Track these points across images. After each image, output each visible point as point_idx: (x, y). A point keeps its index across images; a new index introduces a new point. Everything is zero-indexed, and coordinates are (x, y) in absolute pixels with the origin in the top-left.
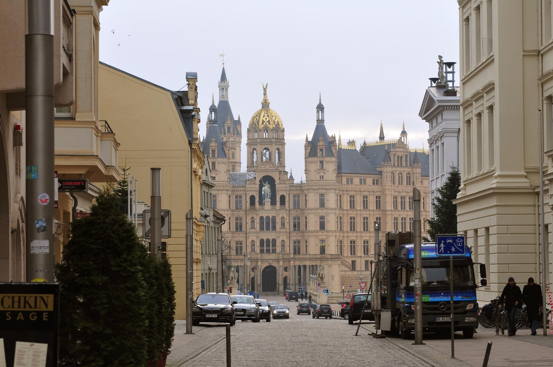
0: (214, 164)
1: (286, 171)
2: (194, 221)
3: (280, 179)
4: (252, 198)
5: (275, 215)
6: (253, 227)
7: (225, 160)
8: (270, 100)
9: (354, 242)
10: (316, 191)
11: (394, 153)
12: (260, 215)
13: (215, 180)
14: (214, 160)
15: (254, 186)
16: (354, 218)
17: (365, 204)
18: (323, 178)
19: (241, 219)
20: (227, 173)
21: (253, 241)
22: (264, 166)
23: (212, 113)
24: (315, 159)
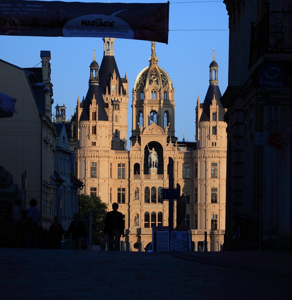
0: (95, 129)
1: (175, 137)
2: (43, 184)
4: (137, 166)
7: (106, 123)
12: (145, 186)
13: (95, 145)
18: (216, 145)
23: (93, 71)
24: (206, 123)
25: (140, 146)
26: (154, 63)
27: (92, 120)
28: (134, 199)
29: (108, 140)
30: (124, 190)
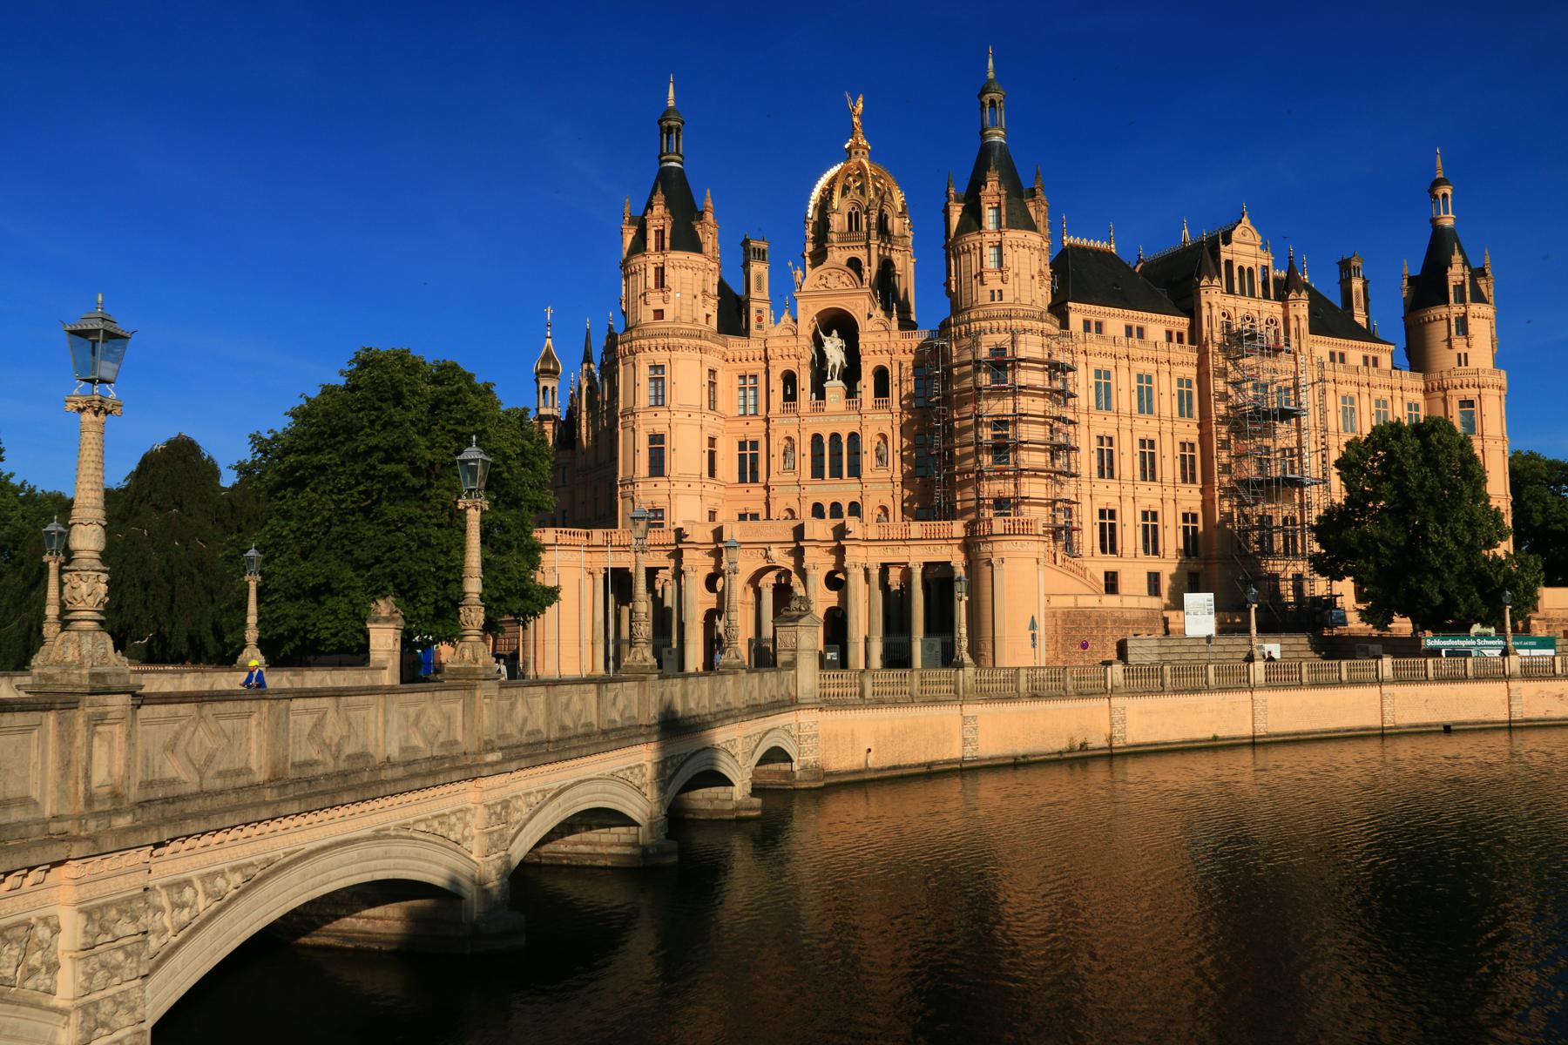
0: (660, 273)
3: (870, 316)
4: (790, 379)
9: (1112, 514)
11: (1229, 257)
15: (793, 341)
16: (1110, 439)
17: (1146, 401)
19: (754, 445)
20: (704, 301)
22: (824, 281)
24: (972, 239)
25: (794, 324)
26: (856, 153)
27: (653, 250)
28: (781, 469)
29: (701, 304)
30: (754, 445)
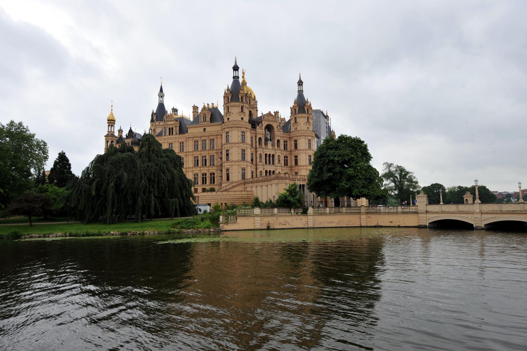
0: (242, 107)
3: (277, 128)
5: (274, 153)
6: (261, 161)
8: (246, 81)
10: (306, 137)
12: (265, 153)
14: (243, 104)
15: (261, 131)
21: (261, 172)
22: (268, 117)
